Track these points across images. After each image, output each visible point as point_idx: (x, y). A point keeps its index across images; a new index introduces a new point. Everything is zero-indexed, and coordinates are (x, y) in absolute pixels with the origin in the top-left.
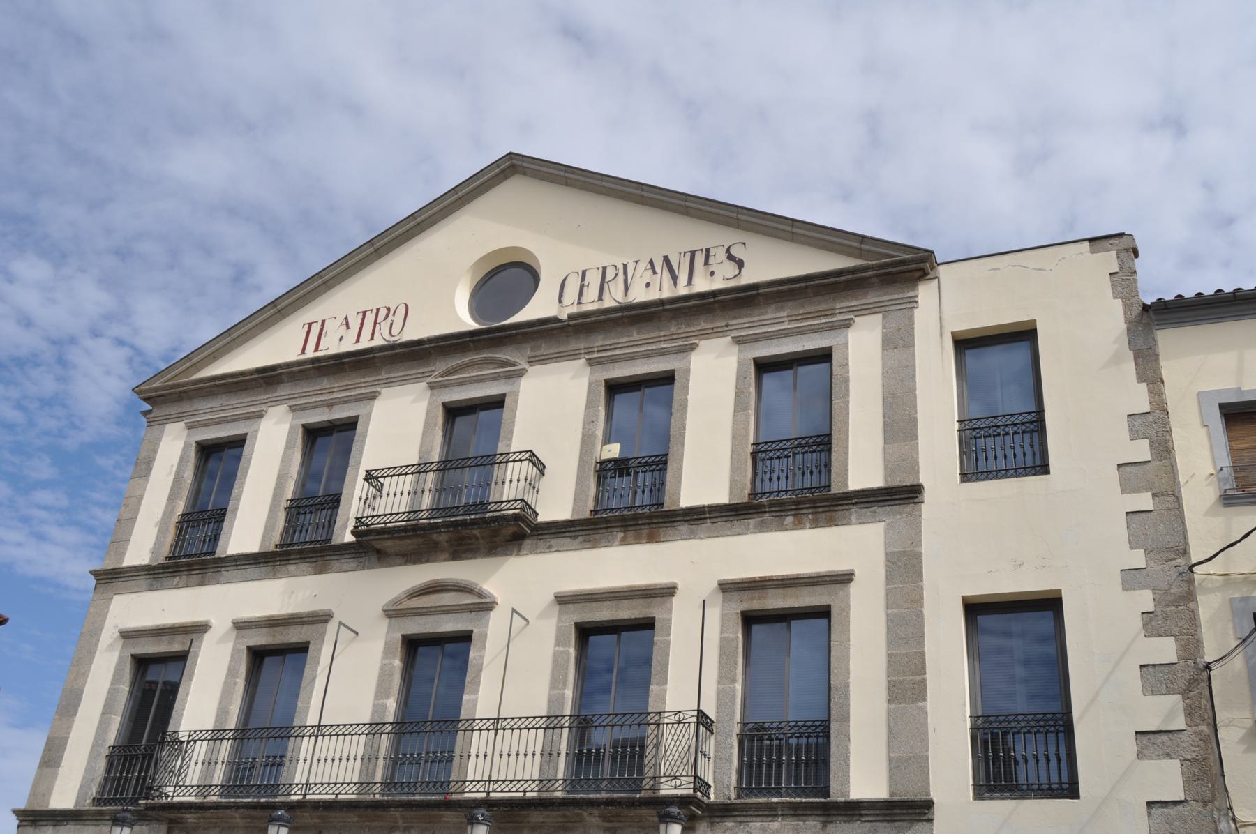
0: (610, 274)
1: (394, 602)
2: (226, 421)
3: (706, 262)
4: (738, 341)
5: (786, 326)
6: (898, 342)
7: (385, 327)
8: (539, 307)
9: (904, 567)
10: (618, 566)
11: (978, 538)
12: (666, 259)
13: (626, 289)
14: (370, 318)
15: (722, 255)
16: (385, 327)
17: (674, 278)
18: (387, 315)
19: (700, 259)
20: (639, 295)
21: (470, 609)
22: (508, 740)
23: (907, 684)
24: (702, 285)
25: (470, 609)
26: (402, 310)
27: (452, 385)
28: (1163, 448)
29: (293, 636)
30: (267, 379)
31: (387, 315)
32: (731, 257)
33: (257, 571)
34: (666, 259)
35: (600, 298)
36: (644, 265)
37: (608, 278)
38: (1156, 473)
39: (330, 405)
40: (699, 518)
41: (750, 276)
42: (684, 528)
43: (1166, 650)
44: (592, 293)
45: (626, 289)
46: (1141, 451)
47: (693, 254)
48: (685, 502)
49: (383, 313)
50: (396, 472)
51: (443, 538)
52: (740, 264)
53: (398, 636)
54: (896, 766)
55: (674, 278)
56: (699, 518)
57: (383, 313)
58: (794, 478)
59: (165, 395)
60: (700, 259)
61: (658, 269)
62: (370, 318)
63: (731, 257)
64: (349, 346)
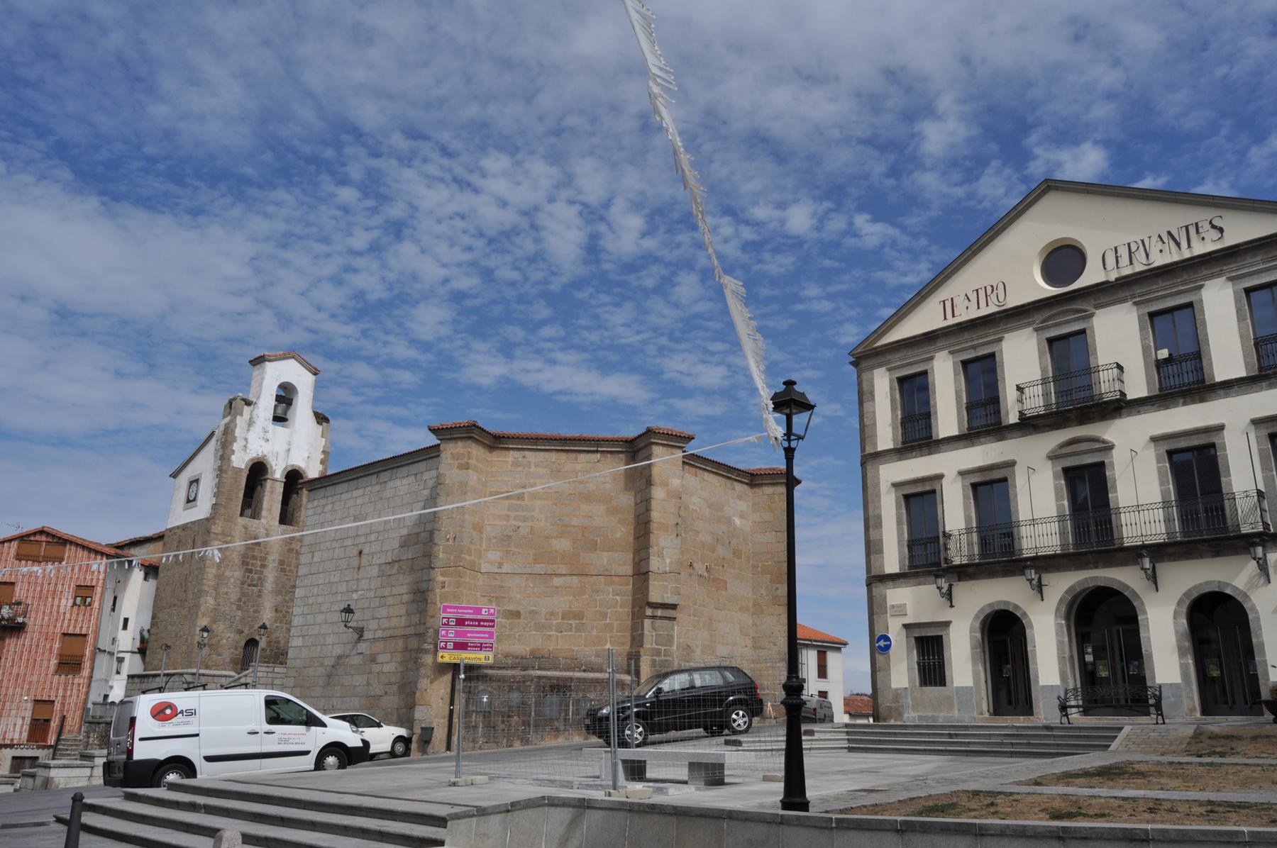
0: (1134, 248)
1: (1052, 451)
2: (911, 364)
3: (1198, 232)
4: (1231, 279)
5: (1262, 266)
7: (993, 297)
8: (1092, 275)
10: (1184, 418)
12: (1169, 233)
13: (1147, 255)
14: (982, 293)
15: (1207, 226)
16: (993, 297)
17: (1178, 244)
19: (1192, 230)
20: (1159, 260)
21: (1100, 450)
22: (1146, 516)
24: (1199, 249)
25: (1100, 450)
26: (1001, 286)
27: (1049, 327)
29: (996, 475)
30: (930, 338)
32: (1214, 227)
33: (961, 444)
34: (1169, 233)
35: (1131, 263)
36: (1155, 239)
37: (1133, 249)
39: (974, 348)
40: (1229, 386)
41: (1231, 239)
42: (1221, 392)
44: (1124, 260)
45: (1147, 255)
47: (1187, 227)
48: (1218, 379)
49: (989, 289)
50: (1032, 384)
51: (1072, 415)
52: (1221, 230)
55: (1178, 244)
56: (1229, 386)
57: (989, 289)
59: (865, 357)
60: (1192, 230)
61: (1165, 239)
62: (982, 293)
63: (1214, 227)
64: (974, 314)
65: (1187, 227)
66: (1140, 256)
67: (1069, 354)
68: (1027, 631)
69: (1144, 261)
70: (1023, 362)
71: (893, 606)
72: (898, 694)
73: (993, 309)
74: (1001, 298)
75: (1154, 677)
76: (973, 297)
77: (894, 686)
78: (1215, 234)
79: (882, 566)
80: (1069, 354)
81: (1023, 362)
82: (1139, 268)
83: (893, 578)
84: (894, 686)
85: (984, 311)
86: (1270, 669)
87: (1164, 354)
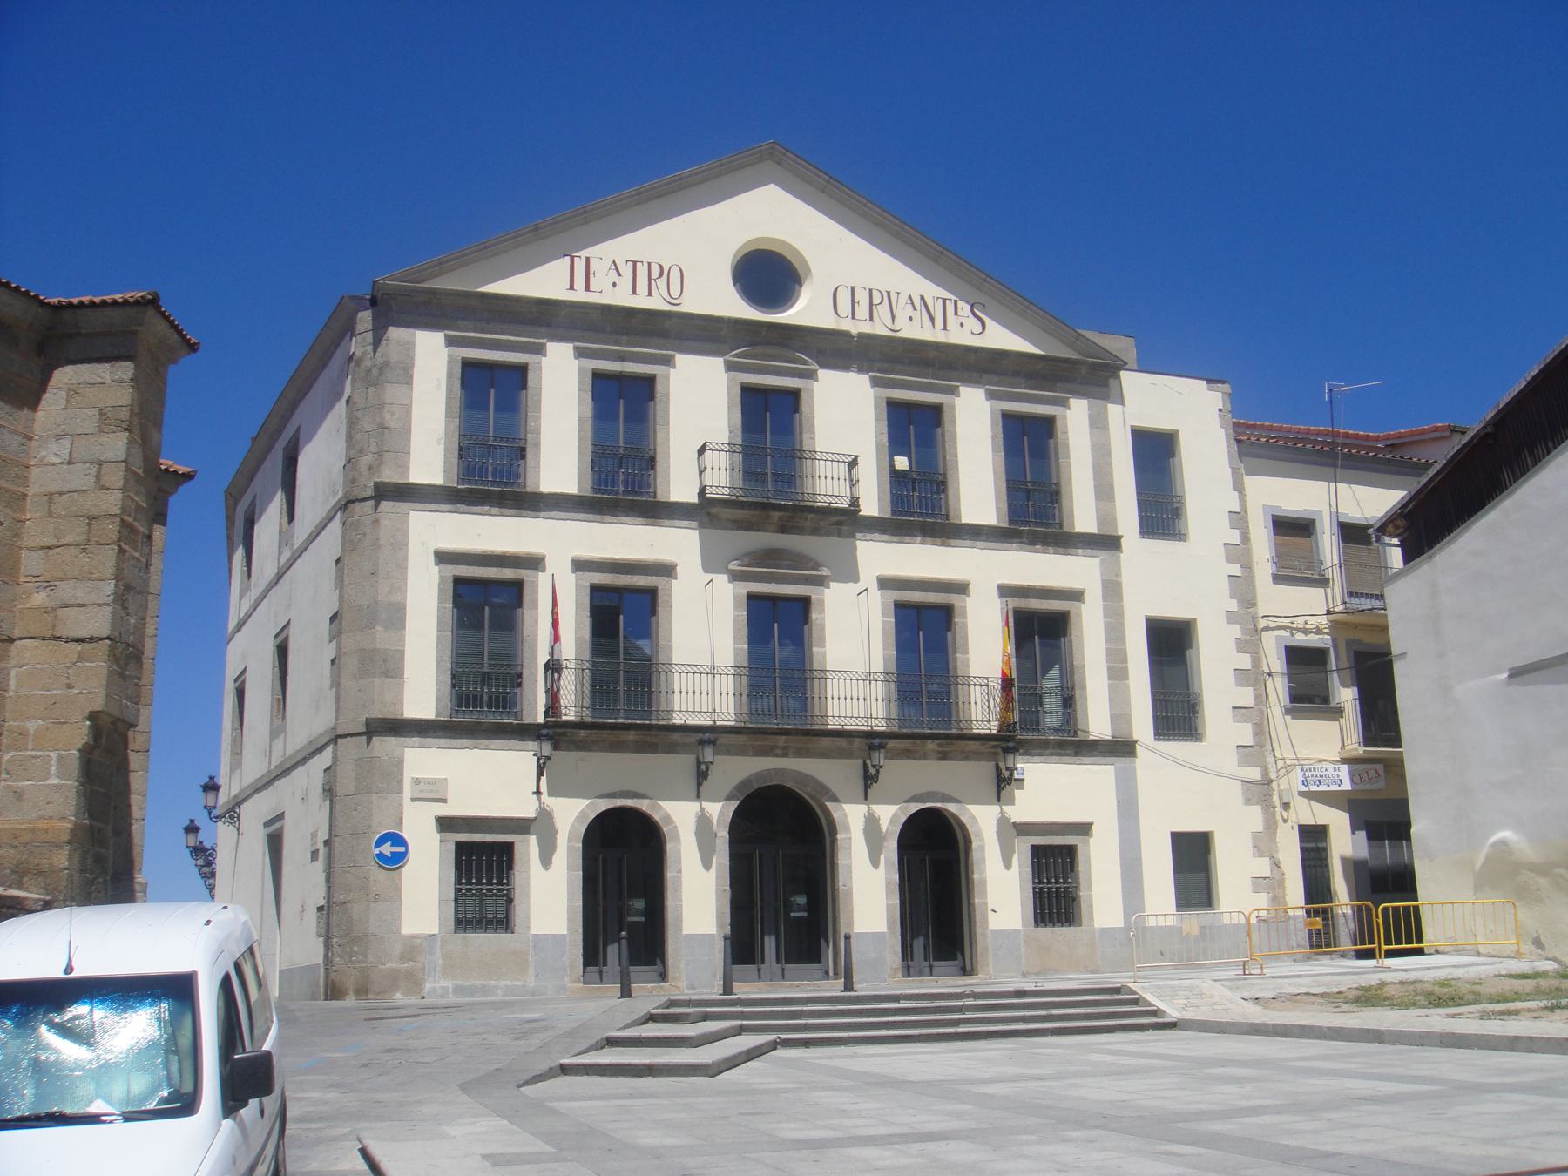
0: (877, 300)
6: (1098, 424)
9: (1112, 590)
11: (1159, 579)
12: (922, 298)
13: (893, 317)
14: (642, 271)
18: (661, 275)
23: (1117, 672)
26: (675, 275)
28: (1245, 538)
31: (661, 275)
34: (922, 298)
35: (871, 319)
36: (904, 299)
38: (1239, 553)
39: (622, 357)
40: (977, 533)
43: (1245, 662)
44: (862, 311)
45: (893, 317)
46: (1235, 537)
49: (655, 272)
53: (744, 592)
54: (1114, 719)
56: (977, 533)
57: (655, 272)
58: (1034, 512)
64: (621, 297)
65: (944, 300)
66: (883, 312)
67: (770, 420)
68: (669, 847)
69: (889, 322)
70: (698, 407)
71: (417, 781)
72: (413, 947)
73: (656, 303)
74: (675, 292)
75: (851, 924)
76: (627, 271)
77: (407, 928)
78: (978, 327)
79: (399, 701)
80: (770, 420)
81: (698, 407)
82: (879, 329)
83: (422, 729)
84: (407, 928)
85: (641, 302)
86: (990, 914)
87: (902, 463)
